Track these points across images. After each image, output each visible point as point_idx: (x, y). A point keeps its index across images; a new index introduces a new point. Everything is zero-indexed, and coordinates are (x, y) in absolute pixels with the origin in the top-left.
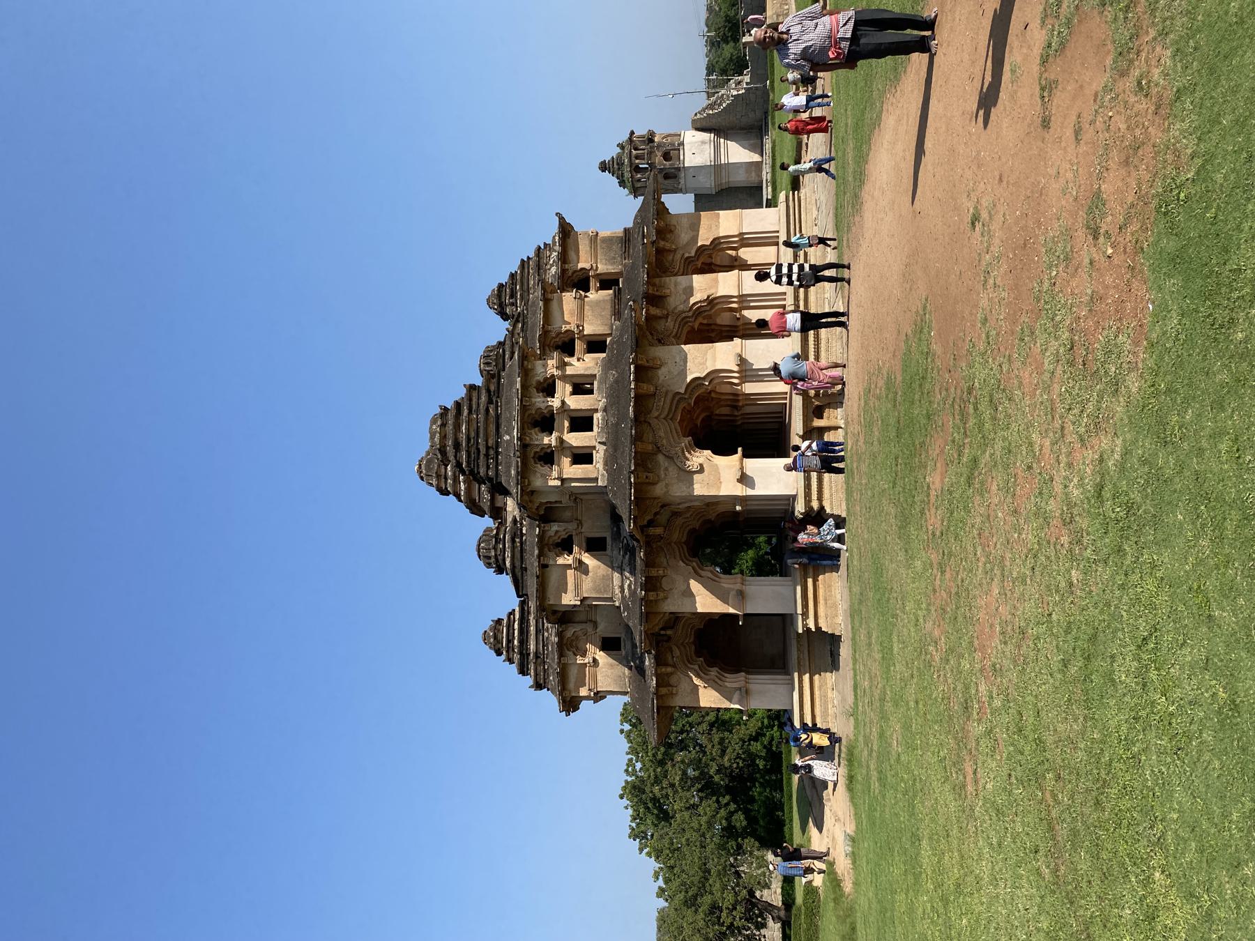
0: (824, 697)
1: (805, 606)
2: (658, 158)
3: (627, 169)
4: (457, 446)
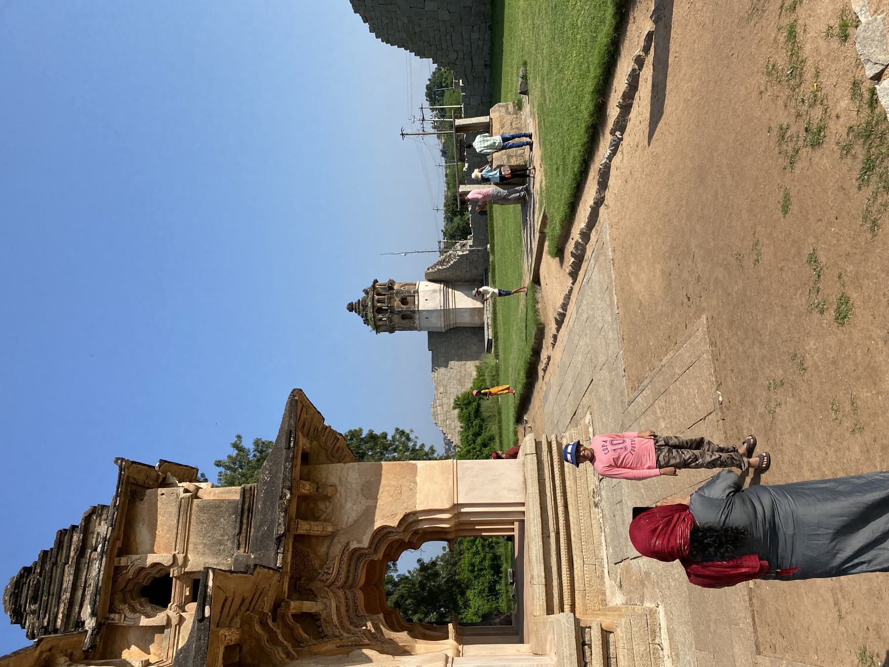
2: (397, 303)
3: (370, 311)
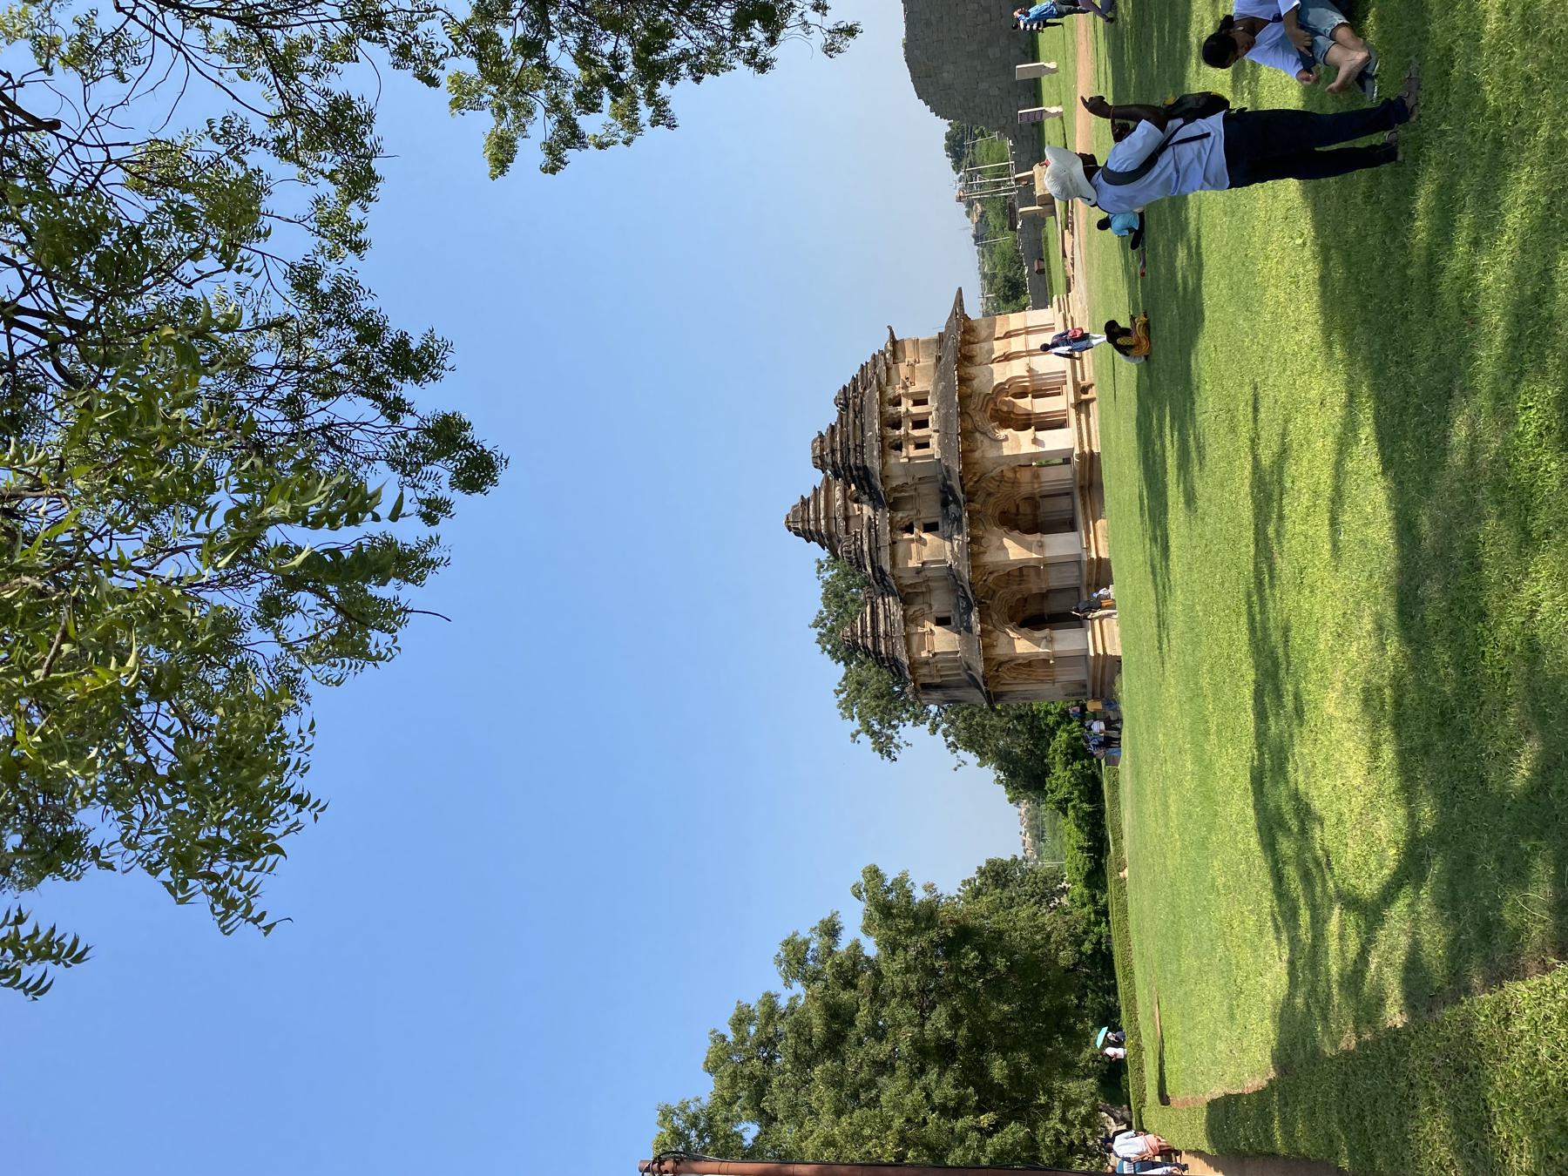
1: (1089, 543)
4: (833, 451)
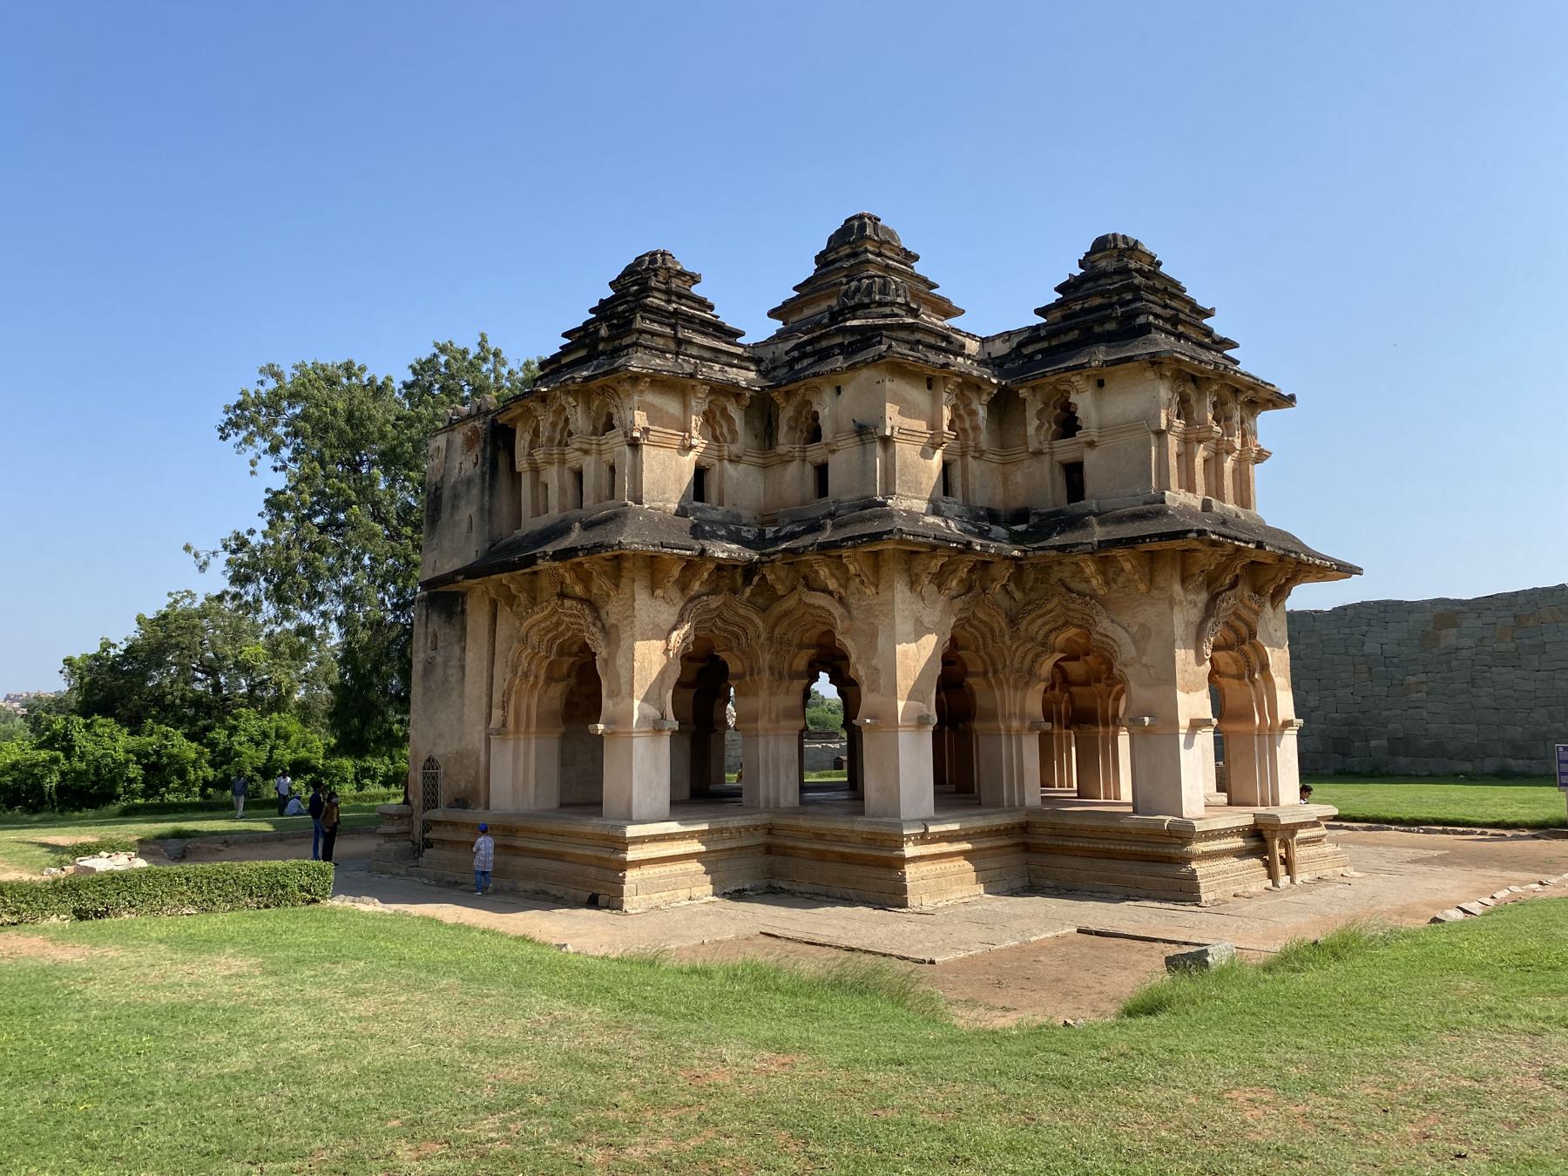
0: (671, 884)
